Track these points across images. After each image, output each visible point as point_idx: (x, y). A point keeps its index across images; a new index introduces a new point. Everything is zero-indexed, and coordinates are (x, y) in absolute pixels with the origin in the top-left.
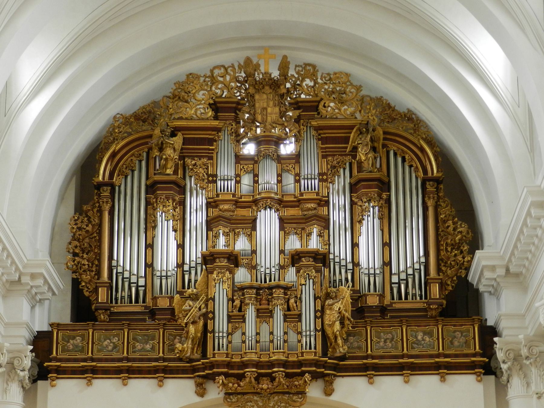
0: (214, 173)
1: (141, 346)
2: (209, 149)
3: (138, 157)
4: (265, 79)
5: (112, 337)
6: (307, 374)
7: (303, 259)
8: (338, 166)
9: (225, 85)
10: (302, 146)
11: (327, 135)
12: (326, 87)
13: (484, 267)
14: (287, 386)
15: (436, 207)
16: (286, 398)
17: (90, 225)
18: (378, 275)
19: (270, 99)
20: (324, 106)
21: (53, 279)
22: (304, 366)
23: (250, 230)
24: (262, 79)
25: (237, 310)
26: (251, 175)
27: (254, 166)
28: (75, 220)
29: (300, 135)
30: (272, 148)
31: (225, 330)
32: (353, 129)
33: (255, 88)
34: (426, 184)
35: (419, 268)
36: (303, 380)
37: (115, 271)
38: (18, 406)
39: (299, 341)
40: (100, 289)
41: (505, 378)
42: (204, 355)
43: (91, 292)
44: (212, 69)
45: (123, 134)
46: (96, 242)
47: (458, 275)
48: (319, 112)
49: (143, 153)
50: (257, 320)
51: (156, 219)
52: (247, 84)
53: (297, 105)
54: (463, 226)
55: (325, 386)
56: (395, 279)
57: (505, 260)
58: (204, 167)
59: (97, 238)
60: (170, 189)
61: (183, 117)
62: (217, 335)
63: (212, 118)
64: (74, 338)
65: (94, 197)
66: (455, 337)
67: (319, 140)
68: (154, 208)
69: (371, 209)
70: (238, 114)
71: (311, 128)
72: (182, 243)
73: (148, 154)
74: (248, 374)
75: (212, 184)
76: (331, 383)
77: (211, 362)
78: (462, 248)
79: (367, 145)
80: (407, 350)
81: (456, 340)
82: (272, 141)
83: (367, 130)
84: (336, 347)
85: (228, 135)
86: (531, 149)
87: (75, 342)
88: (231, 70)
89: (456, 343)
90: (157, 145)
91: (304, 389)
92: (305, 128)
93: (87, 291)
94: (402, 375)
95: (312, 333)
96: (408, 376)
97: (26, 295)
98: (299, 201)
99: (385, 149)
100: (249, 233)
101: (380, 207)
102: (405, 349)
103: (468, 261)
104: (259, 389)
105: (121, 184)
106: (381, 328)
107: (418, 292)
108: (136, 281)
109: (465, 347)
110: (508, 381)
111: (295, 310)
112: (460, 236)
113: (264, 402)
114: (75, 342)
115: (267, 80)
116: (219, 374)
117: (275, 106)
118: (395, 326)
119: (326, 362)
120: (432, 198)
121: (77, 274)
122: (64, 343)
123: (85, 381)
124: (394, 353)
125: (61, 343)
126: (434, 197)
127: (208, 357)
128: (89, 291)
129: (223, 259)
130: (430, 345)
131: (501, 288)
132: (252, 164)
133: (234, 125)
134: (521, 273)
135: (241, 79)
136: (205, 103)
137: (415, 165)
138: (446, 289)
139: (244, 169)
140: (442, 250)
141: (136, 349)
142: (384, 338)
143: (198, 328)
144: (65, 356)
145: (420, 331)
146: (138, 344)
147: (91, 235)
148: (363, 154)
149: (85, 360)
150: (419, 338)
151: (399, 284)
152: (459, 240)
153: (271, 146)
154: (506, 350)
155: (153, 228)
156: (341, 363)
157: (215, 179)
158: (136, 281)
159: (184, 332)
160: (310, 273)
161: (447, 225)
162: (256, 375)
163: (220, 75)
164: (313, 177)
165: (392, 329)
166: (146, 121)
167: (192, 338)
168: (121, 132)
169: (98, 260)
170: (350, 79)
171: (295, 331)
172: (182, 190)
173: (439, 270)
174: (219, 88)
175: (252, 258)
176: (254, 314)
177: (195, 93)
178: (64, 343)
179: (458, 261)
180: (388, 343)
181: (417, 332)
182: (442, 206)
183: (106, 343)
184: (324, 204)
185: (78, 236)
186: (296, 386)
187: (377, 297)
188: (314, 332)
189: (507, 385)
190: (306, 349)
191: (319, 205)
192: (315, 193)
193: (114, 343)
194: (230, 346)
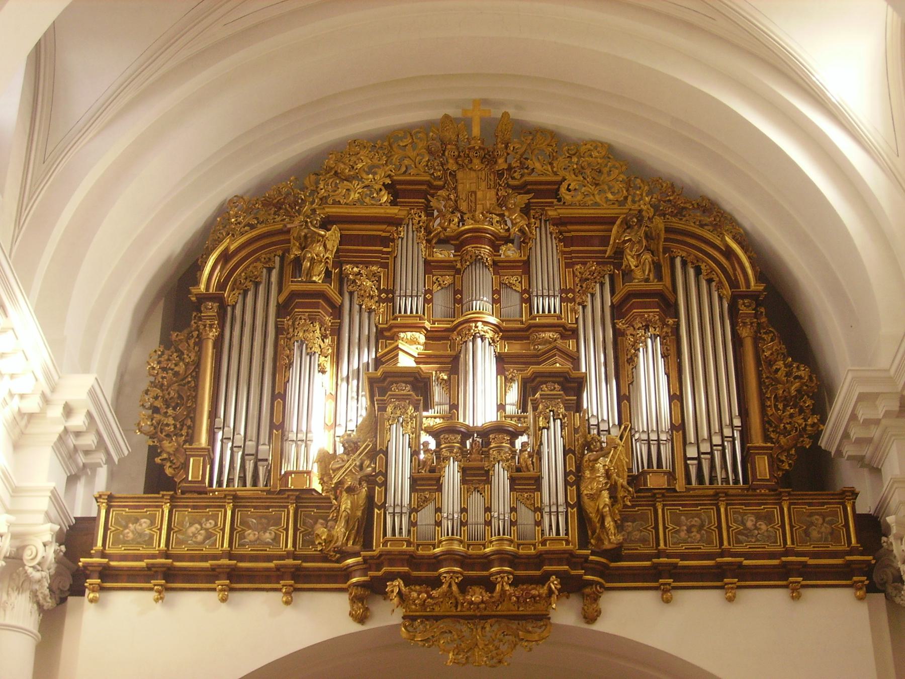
1: (255, 534)
2: (383, 253)
3: (267, 262)
5: (204, 520)
6: (554, 577)
10: (533, 249)
11: (573, 234)
13: (862, 397)
14: (518, 598)
15: (756, 340)
16: (515, 627)
17: (181, 364)
18: (664, 442)
19: (481, 178)
25: (428, 470)
26: (451, 293)
27: (454, 278)
29: (531, 233)
31: (406, 501)
32: (614, 223)
33: (457, 163)
35: (731, 435)
36: (545, 588)
37: (219, 435)
38: (30, 638)
39: (538, 523)
43: (176, 468)
46: (190, 390)
47: (798, 445)
48: (560, 198)
49: (274, 257)
50: (462, 487)
51: (292, 352)
60: (317, 305)
61: (342, 202)
62: (391, 510)
63: (389, 205)
64: (136, 520)
65: (191, 321)
66: (812, 524)
67: (560, 241)
68: (289, 336)
69: (649, 341)
70: (429, 201)
71: (548, 222)
74: (445, 577)
76: (596, 598)
79: (640, 242)
81: (814, 529)
82: (485, 237)
83: (640, 221)
84: (602, 537)
85: (413, 231)
87: (138, 527)
89: (814, 534)
90: (298, 238)
91: (546, 611)
92: (538, 224)
93: (170, 467)
95: (561, 509)
96: (732, 588)
99: (667, 255)
101: (663, 338)
102: (726, 543)
103: (813, 425)
105: (236, 303)
107: (731, 477)
109: (831, 541)
111: (529, 471)
112: (798, 384)
113: (474, 633)
114: (138, 527)
115: (477, 148)
116: (392, 577)
117: (490, 188)
119: (586, 558)
120: (749, 323)
121: (155, 440)
123: (153, 595)
124: (705, 549)
125: (113, 529)
126: (752, 323)
127: (374, 548)
128: (174, 467)
129: (404, 385)
130: (769, 537)
132: (452, 275)
133: (423, 216)
137: (715, 277)
138: (779, 469)
139: (439, 281)
140: (770, 406)
142: (686, 525)
143: (358, 502)
144: (121, 550)
145: (753, 513)
146: (250, 531)
147: (183, 380)
148: (633, 257)
150: (749, 524)
151: (698, 459)
152: (799, 391)
153: (483, 246)
155: (286, 367)
156: (613, 565)
157: (391, 295)
158: (253, 452)
160: (555, 409)
161: (774, 368)
162: (460, 579)
166: (280, 208)
168: (239, 223)
169: (191, 418)
172: (337, 312)
173: (767, 438)
175: (451, 416)
176: (458, 476)
179: (796, 425)
180: (693, 534)
182: (765, 340)
183: (193, 529)
184: (570, 335)
185: (161, 380)
186: (534, 597)
187: (664, 476)
188: (565, 506)
190: (550, 535)
193: (207, 530)
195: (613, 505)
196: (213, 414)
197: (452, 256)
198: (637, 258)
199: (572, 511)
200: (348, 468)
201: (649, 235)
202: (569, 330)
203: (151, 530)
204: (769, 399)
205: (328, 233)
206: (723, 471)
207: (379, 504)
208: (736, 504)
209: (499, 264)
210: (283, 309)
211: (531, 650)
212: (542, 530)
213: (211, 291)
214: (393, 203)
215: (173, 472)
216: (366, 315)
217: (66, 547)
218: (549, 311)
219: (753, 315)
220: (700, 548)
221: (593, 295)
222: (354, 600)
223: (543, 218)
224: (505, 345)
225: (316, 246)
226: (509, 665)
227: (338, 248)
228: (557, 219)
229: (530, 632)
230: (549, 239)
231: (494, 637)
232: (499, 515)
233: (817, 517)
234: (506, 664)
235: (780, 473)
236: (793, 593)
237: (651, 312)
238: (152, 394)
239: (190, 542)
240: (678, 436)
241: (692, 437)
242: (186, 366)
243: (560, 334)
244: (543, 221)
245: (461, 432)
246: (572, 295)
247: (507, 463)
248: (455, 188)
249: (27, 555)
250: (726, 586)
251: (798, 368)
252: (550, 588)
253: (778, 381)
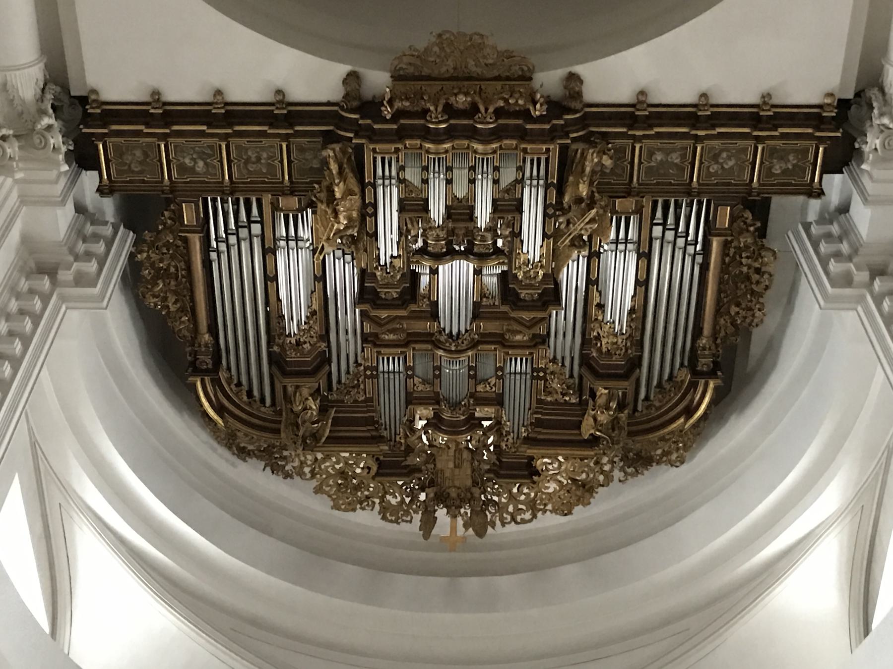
0: (536, 381)
1: (671, 158)
3: (651, 405)
4: (456, 508)
5: (719, 172)
7: (395, 295)
8: (348, 389)
9: (516, 499)
10: (403, 415)
12: (366, 493)
15: (196, 330)
16: (425, 69)
18: (282, 238)
19: (449, 480)
20: (369, 468)
21: (804, 251)
22: (394, 131)
23: (483, 304)
24: (461, 507)
26: (479, 378)
27: (476, 390)
29: (404, 430)
30: (446, 416)
31: (526, 191)
33: (471, 494)
34: (213, 364)
36: (396, 107)
37: (699, 247)
40: (727, 226)
41: (49, 96)
42: (564, 149)
44: (534, 519)
45: (670, 439)
49: (642, 411)
50: (473, 204)
51: (628, 323)
52: (483, 498)
53: (411, 471)
54: (152, 304)
55: (358, 90)
56: (256, 229)
57: (58, 295)
58: (550, 390)
59: (722, 295)
62: (541, 182)
64: (785, 172)
66: (141, 163)
67: (377, 422)
70: (499, 460)
71: (389, 438)
72: (590, 286)
73: (635, 410)
74: (491, 118)
75: (540, 366)
76: (347, 96)
77: (552, 140)
78: (152, 271)
79: (304, 422)
80: (220, 146)
84: (341, 154)
85: (513, 432)
86: (35, 446)
87: (784, 166)
88: (506, 518)
89: (138, 153)
90: (621, 428)
92: (398, 439)
93: (747, 219)
94: (227, 104)
96: (216, 103)
97: (861, 245)
98: (406, 344)
99: (278, 409)
100: (484, 299)
102: (224, 147)
104: (472, 92)
105: (679, 369)
106: (266, 180)
108: (667, 232)
110: (43, 90)
116: (540, 119)
117: (442, 471)
118: (243, 183)
119: (357, 136)
120: (202, 346)
122: (804, 163)
124: (243, 141)
126: (200, 346)
127: (558, 146)
128: (743, 219)
129: (527, 298)
130: (182, 151)
131: (65, 244)
132: (478, 392)
134: (27, 279)
135: (492, 509)
136: (547, 477)
137: (233, 387)
139: (490, 386)
140: (182, 270)
141: (679, 153)
142: (261, 163)
145: (200, 174)
146: (675, 161)
148: (311, 408)
150: (201, 164)
151: (250, 222)
154: (46, 149)
155: (634, 309)
156: (331, 128)
158: (667, 232)
159: (596, 183)
160: (384, 274)
162: (477, 116)
163: (523, 511)
164: (386, 376)
165: (247, 179)
167: (585, 176)
170: (332, 503)
171: (410, 184)
172: (585, 361)
173: (186, 241)
174: (524, 494)
176: (478, 213)
177: (560, 490)
178: (804, 163)
179: (157, 251)
180: (254, 155)
181: (205, 173)
183: (731, 163)
184: (370, 337)
185: (753, 299)
186: (407, 99)
189: (45, 84)
190: (391, 158)
191: (376, 335)
192: (384, 354)
193: (717, 163)
194: (520, 162)
195: (331, 184)
196: (704, 267)
197: (477, 409)
198: (306, 407)
199: (369, 180)
200: (581, 223)
201: (295, 428)
202: (371, 341)
203: (772, 163)
204: (183, 276)
205: (592, 431)
206: (226, 210)
207: (552, 187)
208: (215, 183)
209: (433, 401)
210: (636, 363)
211: (410, 47)
212: (398, 161)
213: (703, 381)
214: (532, 458)
215: (744, 214)
216: (559, 357)
217: (854, 146)
218: (388, 359)
219: (199, 354)
220: (248, 141)
221: (348, 372)
222: (578, 95)
223: (392, 443)
224: (430, 328)
225: (604, 420)
226: (431, 33)
227: (583, 419)
228: (380, 443)
229: (410, 64)
230: (388, 423)
231: (445, 60)
232: (439, 177)
233: (136, 170)
234: (434, 34)
235: (172, 207)
236: (158, 99)
237: (294, 358)
238: (762, 286)
239: (734, 151)
240: (269, 244)
241: (256, 242)
242: (729, 312)
243: (378, 338)
244: (393, 439)
245: (475, 254)
246: (367, 372)
247: (430, 225)
248: (473, 470)
250: (223, 105)
251: (156, 305)
252: (391, 106)
253: (175, 293)
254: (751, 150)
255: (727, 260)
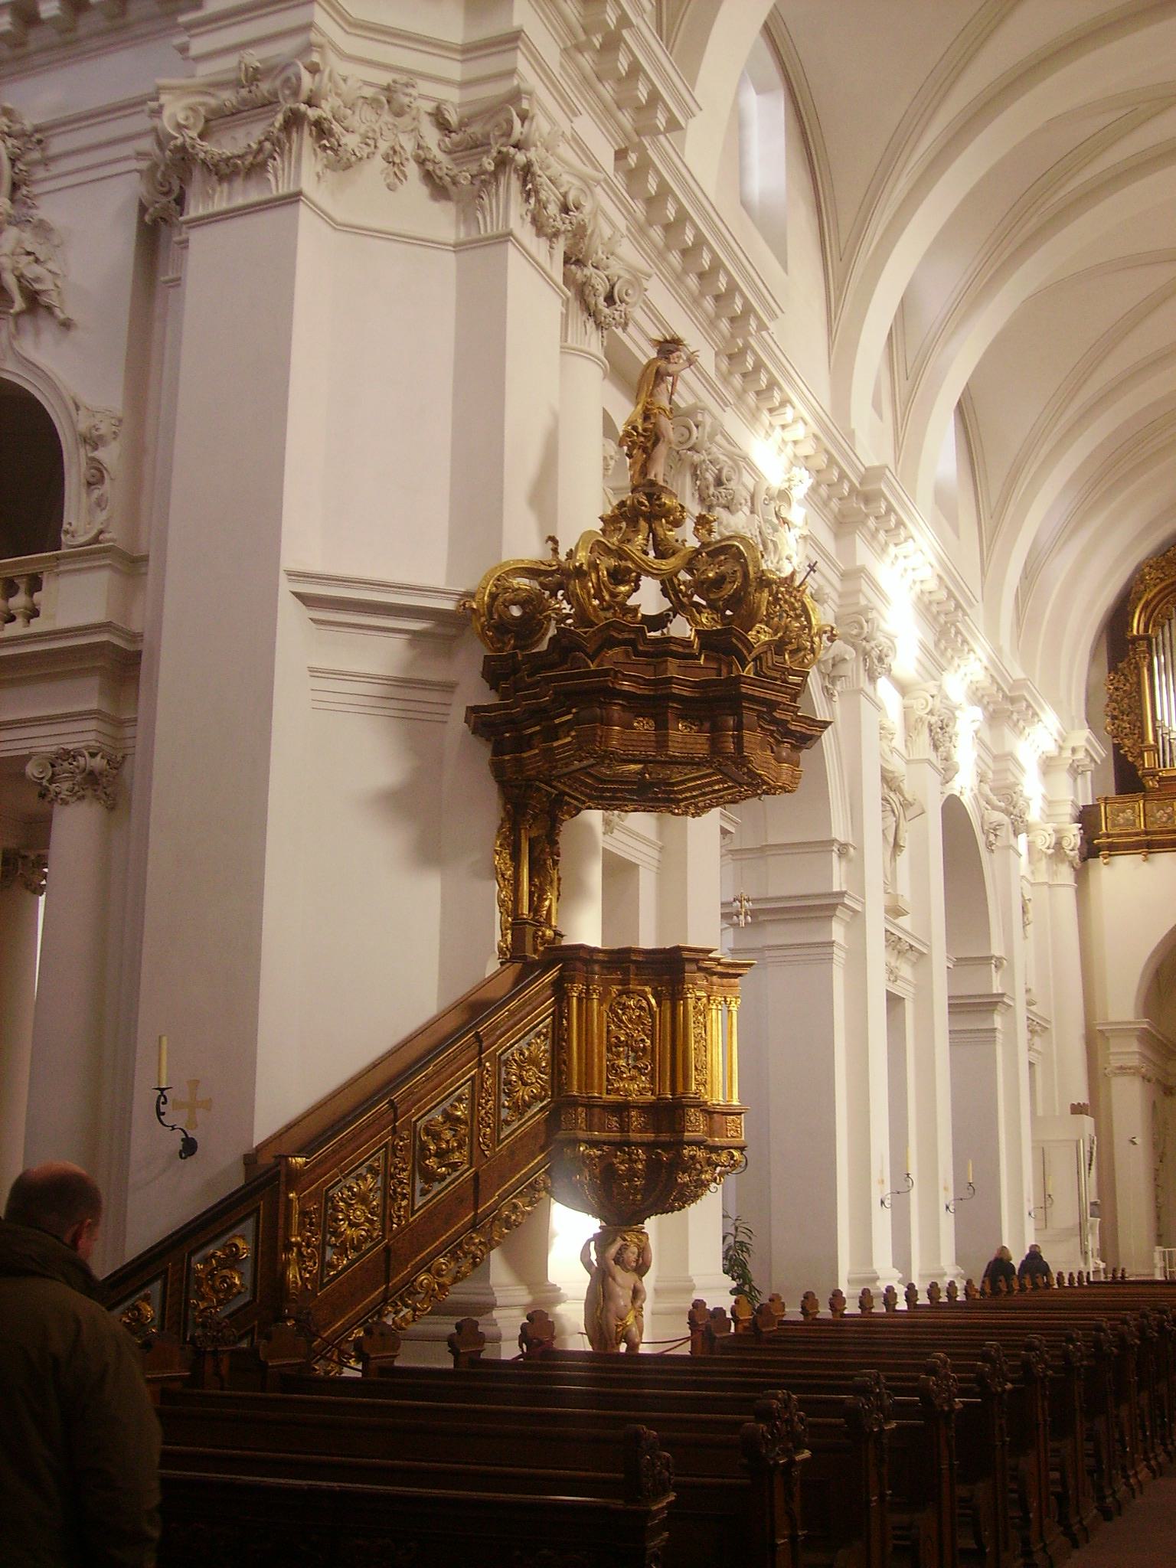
17: (1128, 684)
28: (1111, 680)
37: (1160, 732)
105: (1158, 635)
123: (1141, 856)
144: (1116, 831)
149: (1137, 834)
183: (1158, 814)
249: (1065, 843)
254: (1148, 825)
255: (1139, 724)
